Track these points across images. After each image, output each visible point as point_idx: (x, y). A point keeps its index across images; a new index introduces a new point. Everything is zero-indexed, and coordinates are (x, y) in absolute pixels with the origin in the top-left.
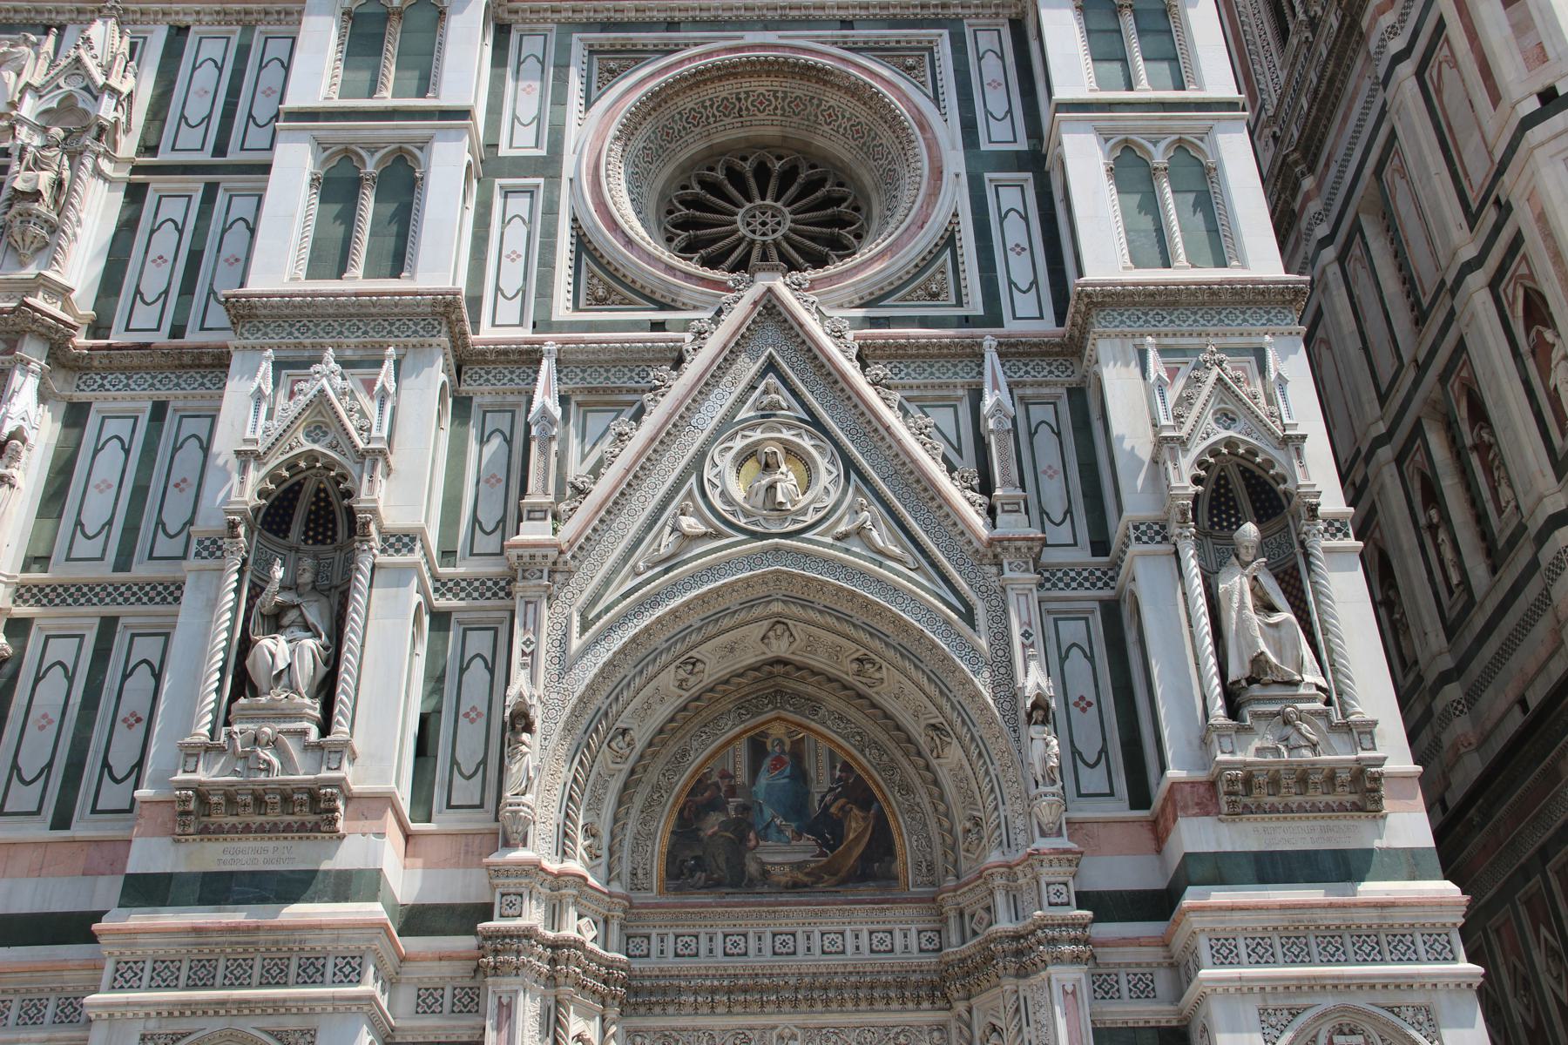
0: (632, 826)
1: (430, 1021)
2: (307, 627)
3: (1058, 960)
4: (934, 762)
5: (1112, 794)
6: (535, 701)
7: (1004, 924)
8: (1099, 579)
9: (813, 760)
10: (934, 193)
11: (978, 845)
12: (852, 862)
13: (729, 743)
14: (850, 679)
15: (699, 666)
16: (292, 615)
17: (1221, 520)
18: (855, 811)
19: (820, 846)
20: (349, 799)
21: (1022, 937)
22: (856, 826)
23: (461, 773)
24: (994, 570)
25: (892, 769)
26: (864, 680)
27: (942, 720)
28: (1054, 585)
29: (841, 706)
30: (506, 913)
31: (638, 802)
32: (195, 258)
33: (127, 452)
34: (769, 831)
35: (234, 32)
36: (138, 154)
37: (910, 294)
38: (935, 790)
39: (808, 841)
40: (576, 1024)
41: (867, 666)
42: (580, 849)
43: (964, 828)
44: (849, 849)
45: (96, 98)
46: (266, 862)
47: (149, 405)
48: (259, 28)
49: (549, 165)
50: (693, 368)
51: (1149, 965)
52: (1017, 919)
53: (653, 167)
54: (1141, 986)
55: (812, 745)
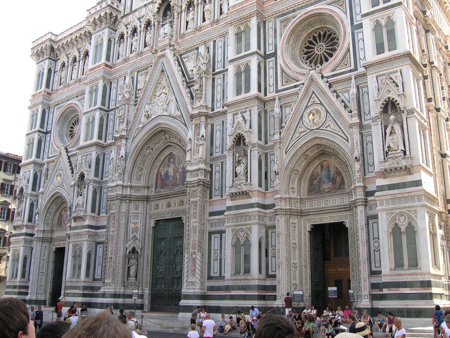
0: (302, 184)
1: (271, 223)
2: (243, 163)
3: (359, 205)
7: (353, 199)
10: (344, 40)
16: (241, 161)
17: (394, 111)
22: (338, 179)
24: (352, 129)
28: (366, 129)
31: (303, 180)
32: (224, 90)
37: (341, 66)
39: (331, 183)
40: (291, 222)
44: (337, 184)
48: (226, 37)
49: (274, 54)
50: (300, 97)
53: (297, 44)
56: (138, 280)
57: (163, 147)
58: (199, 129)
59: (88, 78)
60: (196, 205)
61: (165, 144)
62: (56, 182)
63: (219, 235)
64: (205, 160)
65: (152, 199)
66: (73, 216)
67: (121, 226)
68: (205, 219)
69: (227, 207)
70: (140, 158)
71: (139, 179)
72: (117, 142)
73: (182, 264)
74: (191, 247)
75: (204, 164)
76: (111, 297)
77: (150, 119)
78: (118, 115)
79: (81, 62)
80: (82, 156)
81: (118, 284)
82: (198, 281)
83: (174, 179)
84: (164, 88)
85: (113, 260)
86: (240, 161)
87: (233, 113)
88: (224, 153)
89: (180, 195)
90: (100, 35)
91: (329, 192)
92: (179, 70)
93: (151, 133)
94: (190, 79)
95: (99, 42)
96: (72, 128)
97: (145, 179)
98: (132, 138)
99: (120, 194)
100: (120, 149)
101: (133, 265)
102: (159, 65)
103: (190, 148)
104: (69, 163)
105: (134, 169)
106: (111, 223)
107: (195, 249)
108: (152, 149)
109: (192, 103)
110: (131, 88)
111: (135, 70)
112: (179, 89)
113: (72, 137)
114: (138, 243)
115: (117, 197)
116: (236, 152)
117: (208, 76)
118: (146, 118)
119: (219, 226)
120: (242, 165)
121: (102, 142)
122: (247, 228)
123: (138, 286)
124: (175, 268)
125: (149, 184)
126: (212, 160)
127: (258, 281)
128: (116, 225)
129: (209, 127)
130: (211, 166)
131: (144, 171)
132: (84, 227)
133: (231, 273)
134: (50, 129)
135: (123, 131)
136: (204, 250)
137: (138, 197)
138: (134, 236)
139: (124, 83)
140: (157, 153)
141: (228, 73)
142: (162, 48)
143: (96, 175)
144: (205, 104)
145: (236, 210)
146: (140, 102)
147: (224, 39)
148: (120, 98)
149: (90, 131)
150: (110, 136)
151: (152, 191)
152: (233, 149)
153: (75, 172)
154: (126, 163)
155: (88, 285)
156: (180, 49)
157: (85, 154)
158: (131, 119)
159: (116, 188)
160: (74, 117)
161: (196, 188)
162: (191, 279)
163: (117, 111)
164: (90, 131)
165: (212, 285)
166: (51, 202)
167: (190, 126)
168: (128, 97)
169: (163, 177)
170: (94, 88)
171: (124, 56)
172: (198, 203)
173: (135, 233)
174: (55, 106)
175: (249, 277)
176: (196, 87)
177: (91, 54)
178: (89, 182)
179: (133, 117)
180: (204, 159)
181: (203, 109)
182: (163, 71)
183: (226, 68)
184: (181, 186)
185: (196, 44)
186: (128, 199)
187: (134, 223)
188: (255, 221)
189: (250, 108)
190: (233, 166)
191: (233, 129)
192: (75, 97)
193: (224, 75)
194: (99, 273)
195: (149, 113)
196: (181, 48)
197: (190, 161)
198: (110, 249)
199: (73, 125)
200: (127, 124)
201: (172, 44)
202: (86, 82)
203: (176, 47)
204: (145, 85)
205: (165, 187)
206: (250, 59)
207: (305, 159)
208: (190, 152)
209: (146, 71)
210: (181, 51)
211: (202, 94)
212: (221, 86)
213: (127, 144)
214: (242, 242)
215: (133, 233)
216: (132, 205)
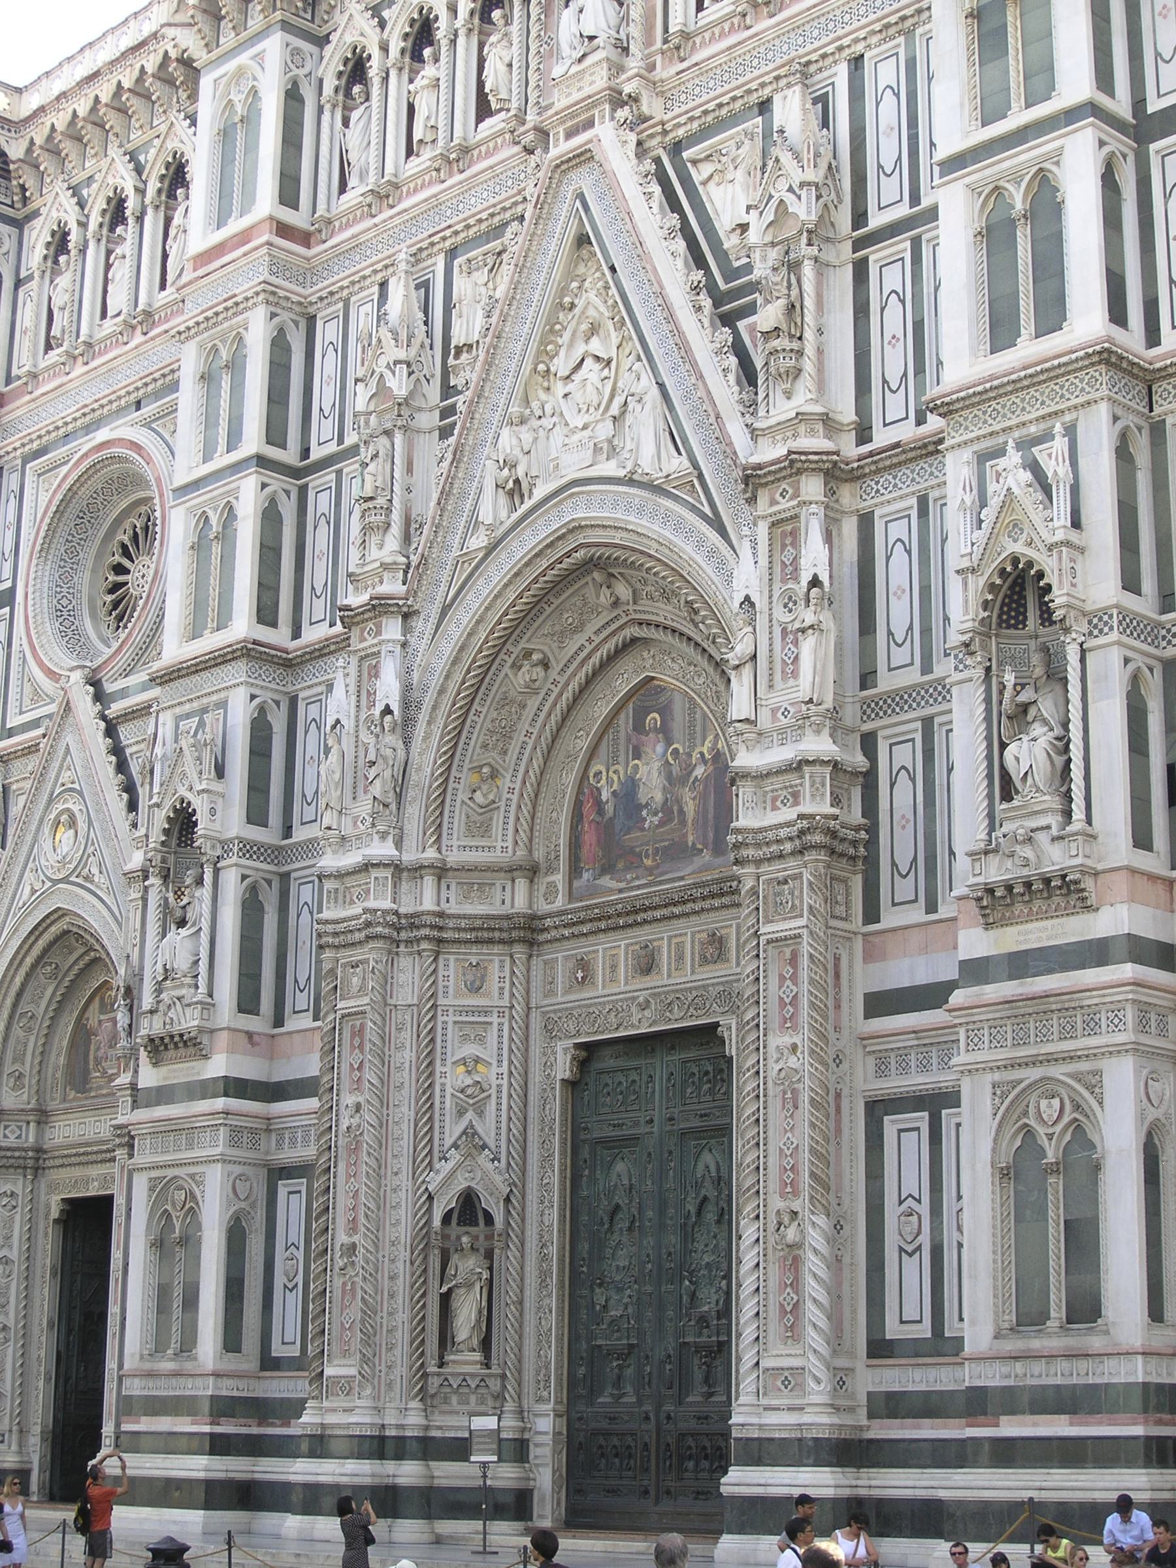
2: (1045, 722)
16: (1032, 712)
20: (1096, 874)
32: (918, 326)
33: (909, 552)
35: (898, 45)
36: (854, 230)
45: (799, 198)
46: (1049, 938)
47: (913, 501)
48: (919, 31)
56: (494, 1361)
57: (604, 651)
58: (795, 544)
59: (189, 305)
60: (794, 960)
61: (613, 633)
62: (53, 858)
63: (926, 1114)
64: (834, 714)
65: (554, 933)
66: (143, 1032)
67: (396, 1078)
68: (845, 1032)
69: (961, 962)
70: (485, 715)
71: (484, 829)
72: (355, 633)
73: (728, 1276)
74: (773, 1185)
75: (826, 731)
76: (360, 1456)
77: (528, 504)
78: (353, 489)
79: (148, 219)
80: (178, 719)
81: (390, 1386)
82: (816, 1366)
83: (671, 820)
84: (594, 330)
85: (359, 1260)
86: (1025, 708)
87: (976, 447)
88: (939, 671)
89: (707, 904)
90: (240, 72)
92: (671, 230)
93: (536, 581)
94: (730, 274)
95: (239, 109)
96: (119, 569)
97: (511, 827)
98: (435, 611)
99: (385, 912)
100: (375, 672)
101: (469, 1286)
102: (564, 208)
103: (750, 650)
104: (113, 759)
105: (454, 773)
106: (345, 1067)
107: (796, 1193)
108: (545, 664)
109: (751, 406)
110: (416, 343)
111: (432, 244)
112: (678, 332)
113: (120, 618)
114: (490, 1166)
115: (368, 924)
116: (1000, 664)
117: (829, 255)
118: (503, 499)
119: (924, 1068)
120: (1038, 730)
121: (279, 637)
122: (1077, 1076)
123: (500, 1397)
124: (693, 1296)
125: (536, 855)
126: (870, 709)
127: (1145, 1363)
128: (369, 1075)
129: (849, 529)
130: (868, 743)
131: (505, 782)
132: (204, 1089)
133: (996, 1321)
134: (8, 584)
135: (386, 575)
136: (846, 1202)
137: (478, 923)
138: (470, 1133)
139: (381, 318)
140: (574, 686)
141: (940, 231)
142: (572, 116)
143: (256, 815)
144: (818, 409)
145: (1011, 977)
146: (471, 414)
147: (910, 44)
148: (361, 398)
149: (214, 581)
150: (319, 605)
151: (552, 889)
152: (985, 647)
153: (143, 803)
154: (407, 742)
155: (235, 1393)
156: (670, 115)
157: (195, 705)
158: (428, 509)
159: (361, 879)
160: (126, 513)
161: (792, 863)
162: (779, 1357)
163: (350, 467)
164: (214, 581)
165: (896, 1388)
166: (29, 961)
167: (746, 531)
168: (404, 392)
169: (609, 809)
170: (224, 354)
171: (372, 172)
172: (805, 948)
173: (470, 1115)
174: (26, 460)
175: (1096, 1343)
176: (769, 315)
177: (200, 174)
178: (219, 852)
179: (435, 496)
180: (829, 703)
181: (812, 433)
182: (582, 240)
183: (925, 202)
184: (707, 856)
185: (754, 85)
186: (427, 938)
187: (463, 1061)
188: (1121, 1038)
189: (1068, 417)
190: (989, 738)
191: (981, 536)
192: (128, 406)
193: (916, 243)
194: (293, 1331)
195: (520, 472)
196: (677, 111)
197: (754, 723)
198: (342, 1201)
199: (126, 553)
200: (407, 539)
201: (628, 89)
202: (178, 322)
203: (651, 106)
204: (494, 320)
205: (620, 865)
206: (1057, 144)
208: (747, 671)
209: (496, 245)
210: (679, 125)
211: (800, 353)
212: (903, 302)
213: (412, 641)
214: (1051, 1157)
215: (461, 1113)
216: (451, 969)
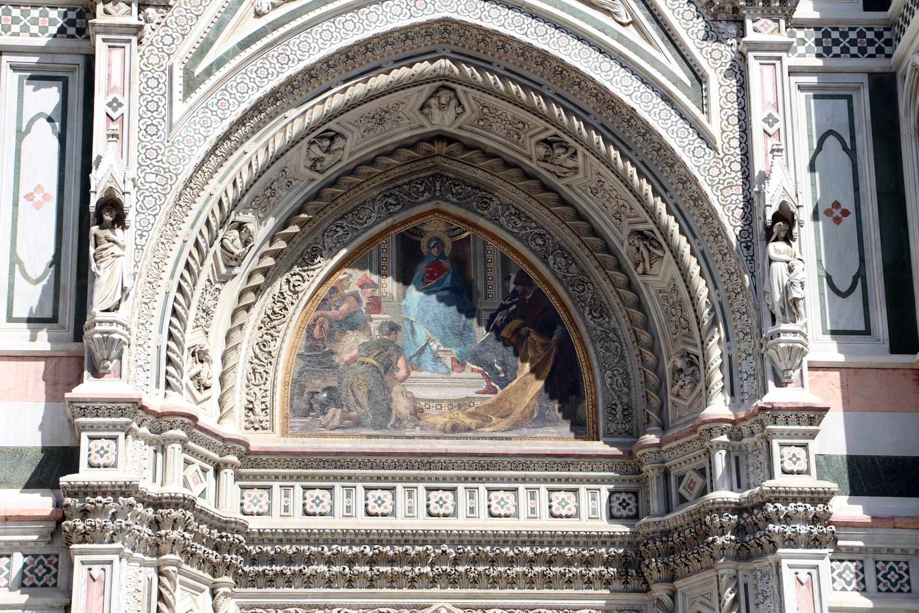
4: (639, 279)
5: (867, 332)
6: (129, 187)
7: (724, 494)
8: (871, 42)
9: (480, 268)
11: (693, 390)
12: (527, 401)
13: (372, 241)
14: (534, 165)
15: (339, 143)
18: (533, 336)
19: (488, 379)
21: (746, 510)
23: (25, 275)
25: (583, 283)
26: (552, 168)
27: (652, 226)
29: (520, 197)
30: (95, 462)
34: (423, 357)
38: (638, 315)
41: (559, 151)
42: (186, 379)
43: (675, 366)
51: (904, 552)
52: (739, 486)
54: (893, 577)
55: (480, 246)
91: (455, 428)
207: (315, 164)
